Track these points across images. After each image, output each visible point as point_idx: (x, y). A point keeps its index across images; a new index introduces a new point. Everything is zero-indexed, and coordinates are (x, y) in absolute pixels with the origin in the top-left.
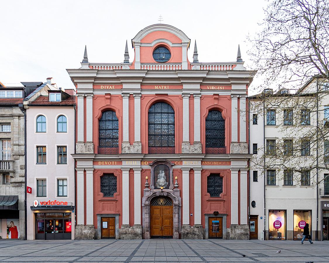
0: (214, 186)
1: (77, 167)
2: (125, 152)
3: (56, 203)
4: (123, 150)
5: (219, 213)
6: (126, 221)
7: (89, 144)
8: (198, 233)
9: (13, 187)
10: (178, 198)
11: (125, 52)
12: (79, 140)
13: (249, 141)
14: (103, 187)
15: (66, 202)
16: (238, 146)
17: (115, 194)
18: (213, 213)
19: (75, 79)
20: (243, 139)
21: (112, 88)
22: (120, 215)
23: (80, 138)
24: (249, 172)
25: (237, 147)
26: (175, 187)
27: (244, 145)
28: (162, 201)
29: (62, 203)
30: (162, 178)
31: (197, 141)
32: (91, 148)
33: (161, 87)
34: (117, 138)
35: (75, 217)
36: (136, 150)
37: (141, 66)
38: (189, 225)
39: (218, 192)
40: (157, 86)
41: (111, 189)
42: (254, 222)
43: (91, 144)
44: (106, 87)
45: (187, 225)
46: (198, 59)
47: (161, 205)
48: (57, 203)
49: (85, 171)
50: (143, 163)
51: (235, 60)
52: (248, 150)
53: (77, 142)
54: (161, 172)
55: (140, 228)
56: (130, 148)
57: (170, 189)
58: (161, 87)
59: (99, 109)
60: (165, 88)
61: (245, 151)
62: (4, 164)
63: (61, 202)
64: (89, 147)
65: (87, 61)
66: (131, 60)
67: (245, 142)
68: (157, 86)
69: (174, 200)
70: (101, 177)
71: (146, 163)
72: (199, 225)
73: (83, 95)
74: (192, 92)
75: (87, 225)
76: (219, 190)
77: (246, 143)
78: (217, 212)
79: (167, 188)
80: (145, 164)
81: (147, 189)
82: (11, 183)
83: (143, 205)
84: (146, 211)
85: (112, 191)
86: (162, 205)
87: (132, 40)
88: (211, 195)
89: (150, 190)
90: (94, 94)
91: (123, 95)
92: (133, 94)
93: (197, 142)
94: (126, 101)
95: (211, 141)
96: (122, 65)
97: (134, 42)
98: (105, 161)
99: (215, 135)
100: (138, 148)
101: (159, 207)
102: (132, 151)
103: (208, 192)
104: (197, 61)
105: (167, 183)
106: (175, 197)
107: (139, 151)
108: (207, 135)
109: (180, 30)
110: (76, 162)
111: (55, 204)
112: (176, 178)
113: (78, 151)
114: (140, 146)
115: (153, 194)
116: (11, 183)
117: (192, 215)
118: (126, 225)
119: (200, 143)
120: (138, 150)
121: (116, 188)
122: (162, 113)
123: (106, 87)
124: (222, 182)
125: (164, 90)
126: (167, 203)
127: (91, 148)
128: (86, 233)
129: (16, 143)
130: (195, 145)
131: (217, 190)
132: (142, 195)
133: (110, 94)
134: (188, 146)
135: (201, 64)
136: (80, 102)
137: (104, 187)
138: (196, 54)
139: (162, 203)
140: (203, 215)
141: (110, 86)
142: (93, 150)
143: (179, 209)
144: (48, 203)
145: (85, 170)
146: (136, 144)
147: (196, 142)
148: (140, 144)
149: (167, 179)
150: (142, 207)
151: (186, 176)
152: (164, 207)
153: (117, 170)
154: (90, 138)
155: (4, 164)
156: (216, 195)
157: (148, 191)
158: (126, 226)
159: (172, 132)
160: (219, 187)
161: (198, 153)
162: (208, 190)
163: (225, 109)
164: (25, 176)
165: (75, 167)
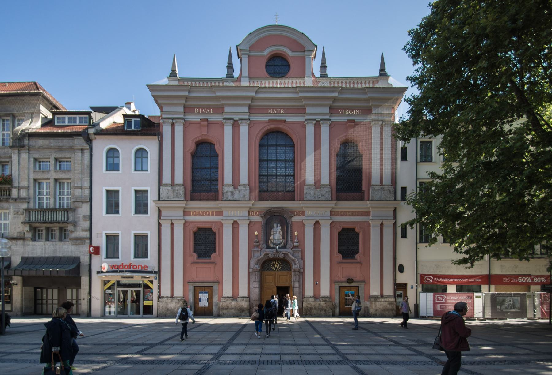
1: (162, 218)
2: (227, 198)
4: (224, 196)
6: (227, 291)
7: (178, 188)
9: (73, 245)
13: (396, 183)
15: (146, 266)
16: (380, 190)
23: (166, 179)
24: (395, 225)
25: (380, 191)
26: (295, 247)
28: (276, 264)
33: (277, 111)
34: (217, 180)
36: (242, 196)
41: (208, 249)
42: (401, 292)
43: (181, 188)
48: (133, 267)
50: (251, 213)
52: (394, 195)
53: (162, 185)
54: (275, 225)
55: (246, 301)
56: (234, 192)
57: (288, 249)
58: (277, 111)
59: (192, 141)
61: (390, 197)
62: (60, 214)
63: (139, 266)
64: (178, 191)
66: (236, 75)
69: (293, 263)
71: (256, 213)
73: (170, 121)
74: (318, 118)
76: (354, 250)
77: (392, 186)
79: (284, 247)
80: (253, 215)
81: (256, 249)
82: (71, 239)
83: (251, 270)
84: (254, 278)
86: (277, 271)
87: (237, 46)
88: (343, 256)
89: (261, 250)
90: (186, 120)
91: (224, 121)
92: (238, 119)
94: (228, 130)
97: (240, 50)
101: (273, 273)
105: (284, 240)
106: (293, 260)
109: (303, 33)
110: (159, 211)
112: (296, 233)
114: (247, 190)
116: (71, 239)
119: (329, 186)
120: (244, 196)
121: (215, 247)
122: (277, 146)
124: (358, 239)
129: (79, 185)
130: (322, 188)
132: (250, 258)
133: (207, 120)
134: (312, 191)
136: (166, 129)
138: (324, 66)
139: (276, 267)
140: (333, 282)
141: (207, 108)
142: (183, 196)
143: (299, 276)
146: (242, 188)
148: (248, 187)
149: (285, 236)
150: (249, 273)
151: (309, 232)
152: (279, 273)
153: (215, 223)
154: (179, 179)
155: (60, 214)
156: (350, 256)
157: (258, 251)
162: (339, 249)
165: (159, 218)
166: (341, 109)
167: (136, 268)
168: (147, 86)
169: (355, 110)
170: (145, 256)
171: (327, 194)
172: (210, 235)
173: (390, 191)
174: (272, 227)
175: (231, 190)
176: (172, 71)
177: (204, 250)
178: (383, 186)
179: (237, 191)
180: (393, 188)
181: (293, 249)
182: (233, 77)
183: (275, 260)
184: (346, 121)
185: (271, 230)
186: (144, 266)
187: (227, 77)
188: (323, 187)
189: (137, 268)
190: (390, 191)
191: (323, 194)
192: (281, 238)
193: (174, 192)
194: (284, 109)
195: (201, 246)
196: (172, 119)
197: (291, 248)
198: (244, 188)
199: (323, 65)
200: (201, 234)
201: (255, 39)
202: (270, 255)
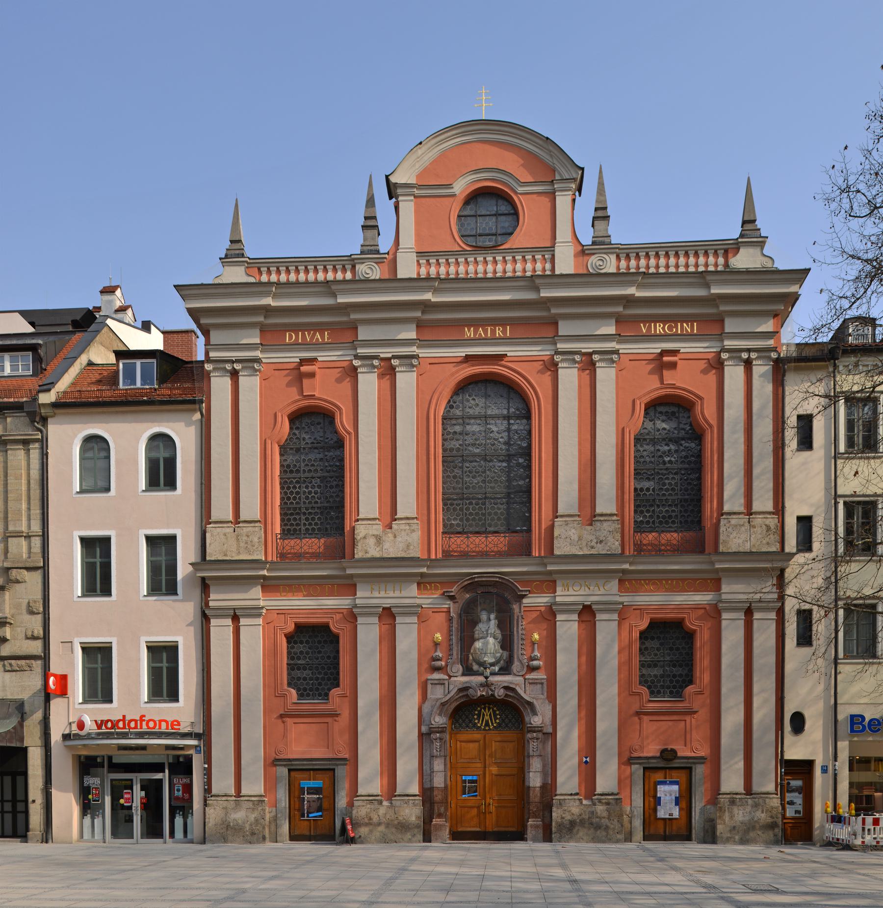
1: (211, 604)
3: (144, 723)
5: (680, 754)
8: (607, 821)
11: (366, 218)
12: (215, 515)
14: (293, 669)
18: (658, 754)
21: (323, 337)
22: (353, 761)
23: (221, 508)
27: (768, 522)
28: (487, 714)
29: (164, 725)
30: (491, 640)
33: (486, 332)
36: (401, 546)
37: (418, 261)
38: (577, 794)
39: (677, 681)
40: (472, 329)
44: (304, 336)
45: (571, 795)
46: (610, 233)
47: (485, 730)
49: (236, 618)
51: (733, 231)
54: (484, 616)
56: (384, 538)
57: (515, 675)
58: (486, 332)
60: (499, 332)
61: (768, 543)
63: (160, 721)
64: (248, 536)
65: (241, 252)
66: (385, 244)
67: (770, 513)
68: (472, 329)
73: (228, 367)
75: (244, 796)
77: (773, 513)
78: (674, 751)
79: (506, 669)
85: (323, 683)
86: (490, 729)
87: (387, 177)
91: (356, 363)
93: (606, 515)
95: (653, 511)
96: (356, 261)
99: (667, 490)
100: (408, 538)
101: (477, 736)
102: (391, 550)
103: (643, 680)
104: (607, 240)
105: (506, 654)
107: (412, 547)
108: (642, 490)
111: (141, 728)
114: (414, 531)
118: (369, 796)
120: (408, 546)
123: (304, 336)
125: (494, 341)
126: (503, 721)
127: (256, 540)
128: (240, 822)
130: (598, 524)
134: (573, 531)
135: (619, 248)
136: (220, 386)
138: (601, 215)
139: (487, 722)
141: (315, 331)
144: (121, 724)
145: (235, 613)
146: (403, 527)
148: (417, 525)
149: (507, 643)
154: (251, 508)
157: (441, 683)
158: (372, 799)
159: (521, 483)
160: (681, 666)
161: (609, 553)
164: (46, 639)
166: (644, 322)
167: (154, 727)
168: (175, 286)
169: (682, 322)
170: (173, 696)
171: (610, 538)
172: (325, 642)
173: (768, 528)
174: (475, 622)
175: (375, 533)
176: (232, 242)
177: (311, 679)
178: (751, 514)
179: (390, 535)
180: (777, 520)
182: (378, 252)
183: (484, 704)
184: (659, 351)
185: (475, 627)
186: (173, 722)
187: (362, 253)
188: (600, 521)
189: (157, 727)
190: (768, 528)
192: (498, 647)
193: (238, 540)
194: (504, 325)
195: (305, 669)
196: (233, 362)
197: (524, 673)
198: (407, 527)
199: (600, 213)
200: (304, 640)
201: (430, 154)
202: (471, 691)
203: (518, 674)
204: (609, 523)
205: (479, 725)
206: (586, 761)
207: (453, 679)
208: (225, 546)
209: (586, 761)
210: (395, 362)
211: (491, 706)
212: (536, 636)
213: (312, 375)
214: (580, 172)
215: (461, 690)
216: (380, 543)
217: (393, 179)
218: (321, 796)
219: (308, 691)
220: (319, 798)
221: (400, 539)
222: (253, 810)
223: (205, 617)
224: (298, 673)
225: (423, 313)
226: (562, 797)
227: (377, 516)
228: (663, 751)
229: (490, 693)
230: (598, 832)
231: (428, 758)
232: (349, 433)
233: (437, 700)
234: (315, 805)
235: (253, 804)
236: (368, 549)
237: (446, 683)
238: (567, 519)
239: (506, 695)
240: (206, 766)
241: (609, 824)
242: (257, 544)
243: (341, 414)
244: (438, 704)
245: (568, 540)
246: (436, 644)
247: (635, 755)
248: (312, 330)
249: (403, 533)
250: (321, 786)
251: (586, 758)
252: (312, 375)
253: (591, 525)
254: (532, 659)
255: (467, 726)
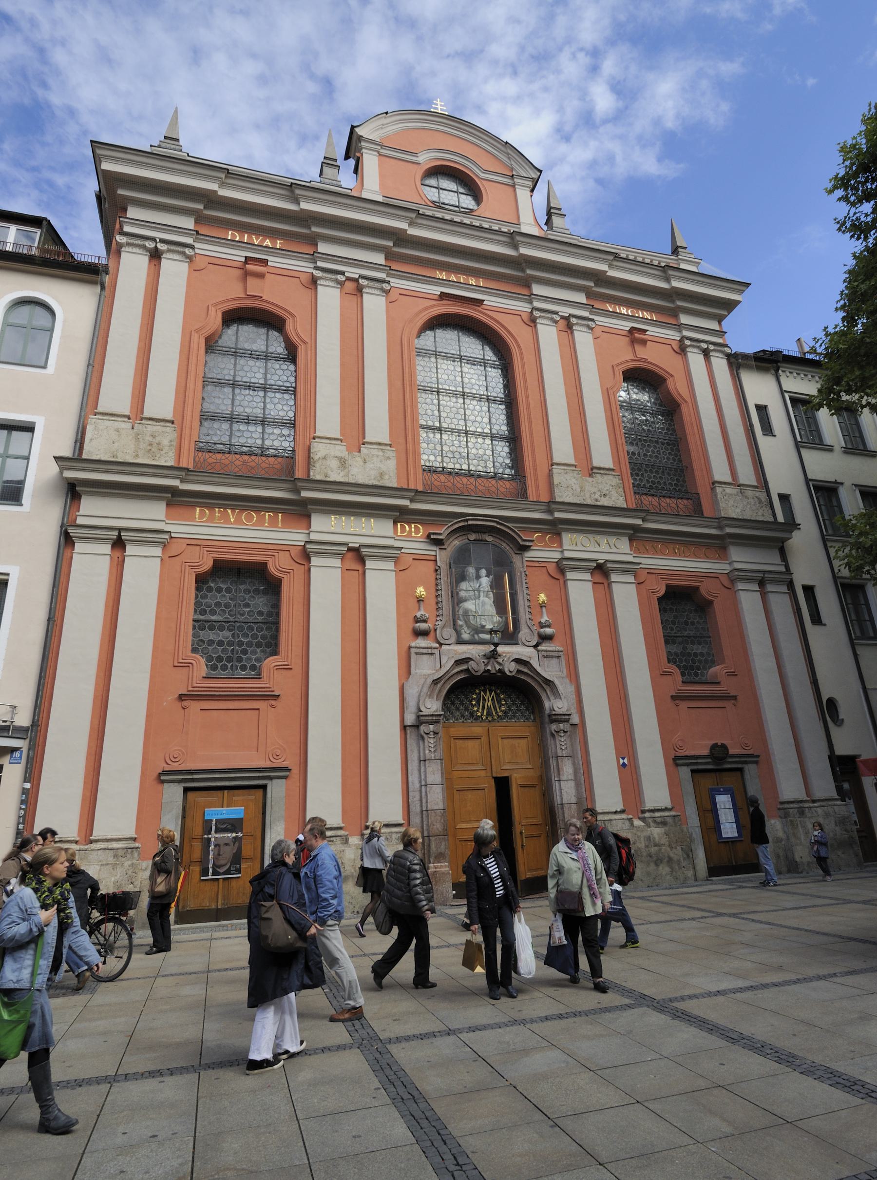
0: (680, 639)
8: (669, 849)
10: (564, 687)
17: (271, 662)
19: (123, 187)
20: (747, 475)
24: (791, 585)
28: (489, 698)
31: (602, 466)
32: (165, 442)
35: (25, 791)
38: (623, 811)
45: (616, 812)
49: (119, 544)
50: (403, 528)
56: (350, 462)
64: (154, 437)
70: (201, 580)
72: (666, 809)
75: (97, 841)
78: (724, 746)
87: (353, 127)
91: (318, 274)
98: (225, 507)
101: (478, 729)
107: (387, 477)
113: (94, 449)
114: (389, 458)
115: (452, 667)
117: (624, 765)
120: (381, 475)
126: (509, 708)
127: (165, 442)
131: (696, 655)
134: (574, 480)
137: (212, 628)
139: (489, 709)
147: (600, 468)
163: (672, 376)
171: (614, 492)
175: (339, 454)
176: (166, 137)
181: (539, 648)
183: (484, 685)
190: (760, 502)
191: (604, 492)
193: (137, 439)
198: (381, 453)
201: (394, 127)
203: (527, 644)
204: (610, 477)
205: (479, 714)
206: (624, 762)
207: (444, 647)
208: (116, 444)
209: (624, 762)
210: (362, 282)
211: (493, 688)
212: (542, 597)
213: (261, 276)
214: (539, 174)
215: (458, 662)
216: (345, 468)
217: (359, 131)
218: (240, 835)
219: (224, 662)
220: (235, 838)
221: (372, 466)
222: (114, 866)
223: (67, 540)
224: (212, 635)
225: (394, 245)
226: (606, 817)
227: (338, 436)
228: (714, 747)
229: (498, 667)
230: (661, 868)
231: (416, 763)
232: (305, 342)
233: (426, 676)
234: (228, 853)
235: (115, 856)
236: (330, 473)
237: (436, 652)
238: (566, 468)
239: (519, 671)
240: (28, 786)
241: (672, 855)
242: (167, 448)
243: (295, 322)
244: (429, 681)
245: (570, 489)
246: (420, 600)
247: (681, 753)
248: (261, 235)
249: (375, 459)
250: (242, 816)
251: (623, 759)
252: (261, 276)
253: (590, 475)
254: (542, 625)
255: (463, 716)
